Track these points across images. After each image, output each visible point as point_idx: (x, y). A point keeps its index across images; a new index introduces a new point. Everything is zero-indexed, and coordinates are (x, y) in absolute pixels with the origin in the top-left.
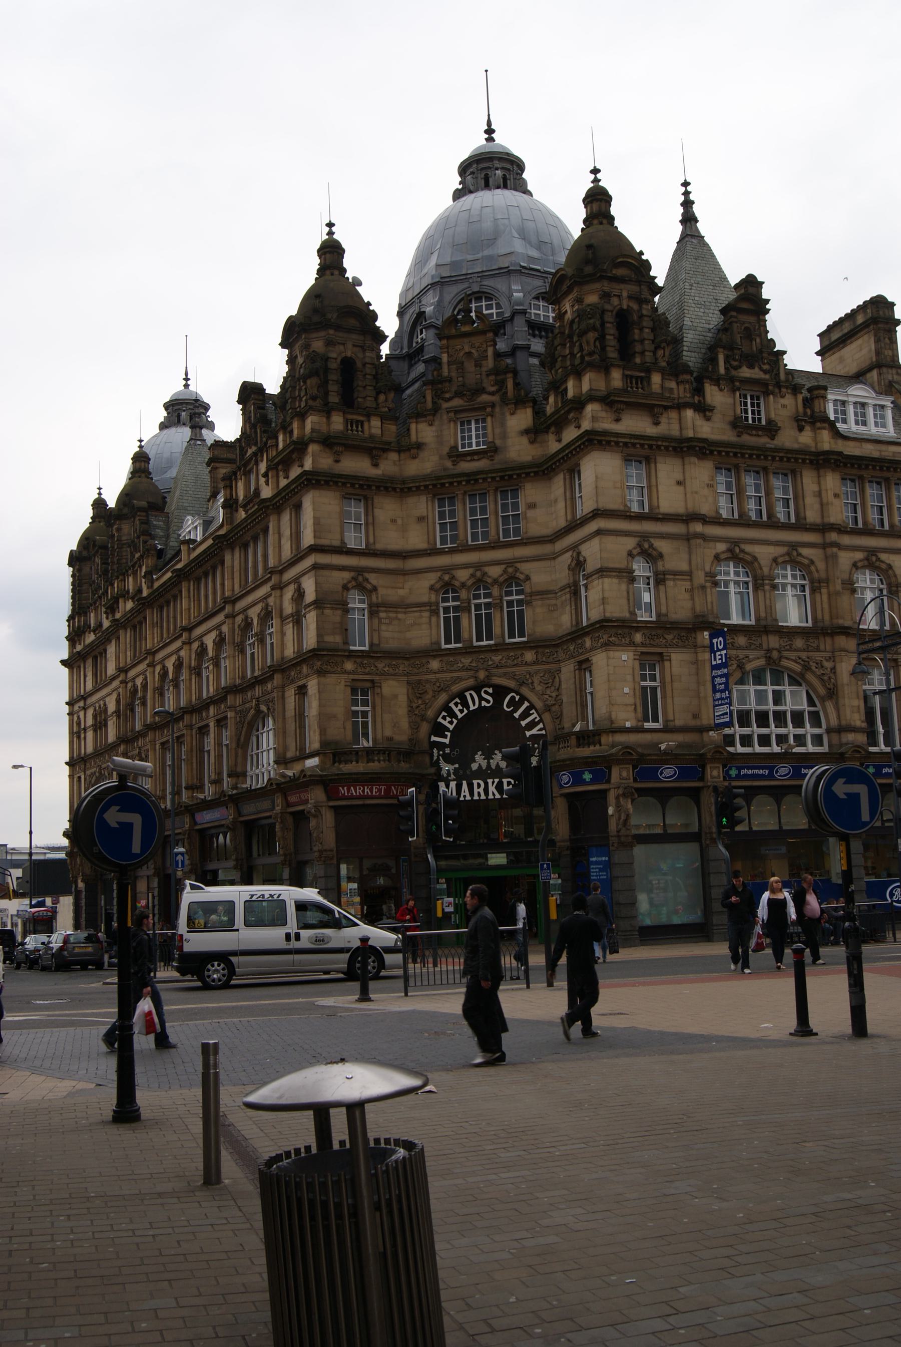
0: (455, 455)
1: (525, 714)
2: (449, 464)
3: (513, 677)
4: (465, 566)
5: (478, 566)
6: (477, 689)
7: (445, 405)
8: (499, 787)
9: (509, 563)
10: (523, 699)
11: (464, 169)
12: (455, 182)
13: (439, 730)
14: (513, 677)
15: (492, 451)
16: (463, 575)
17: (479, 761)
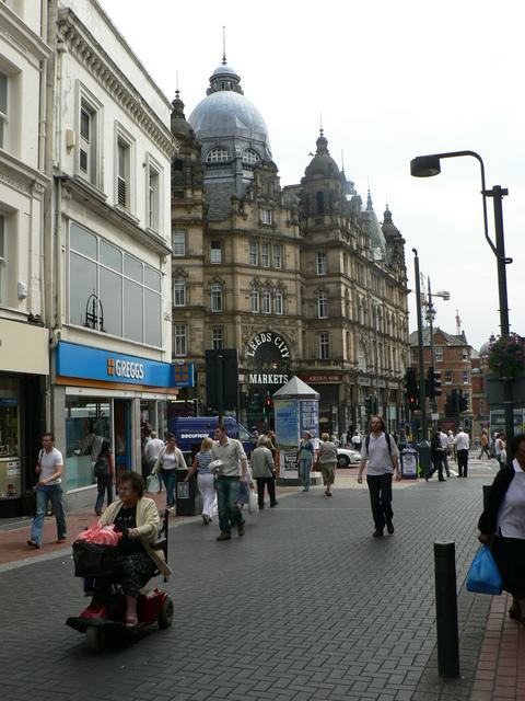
0: (260, 224)
1: (282, 347)
2: (257, 228)
3: (279, 330)
4: (263, 276)
5: (268, 277)
6: (265, 333)
7: (258, 200)
8: (273, 379)
9: (280, 279)
10: (283, 340)
11: (213, 80)
12: (208, 85)
13: (251, 350)
14: (279, 330)
15: (274, 226)
16: (263, 280)
17: (265, 366)
